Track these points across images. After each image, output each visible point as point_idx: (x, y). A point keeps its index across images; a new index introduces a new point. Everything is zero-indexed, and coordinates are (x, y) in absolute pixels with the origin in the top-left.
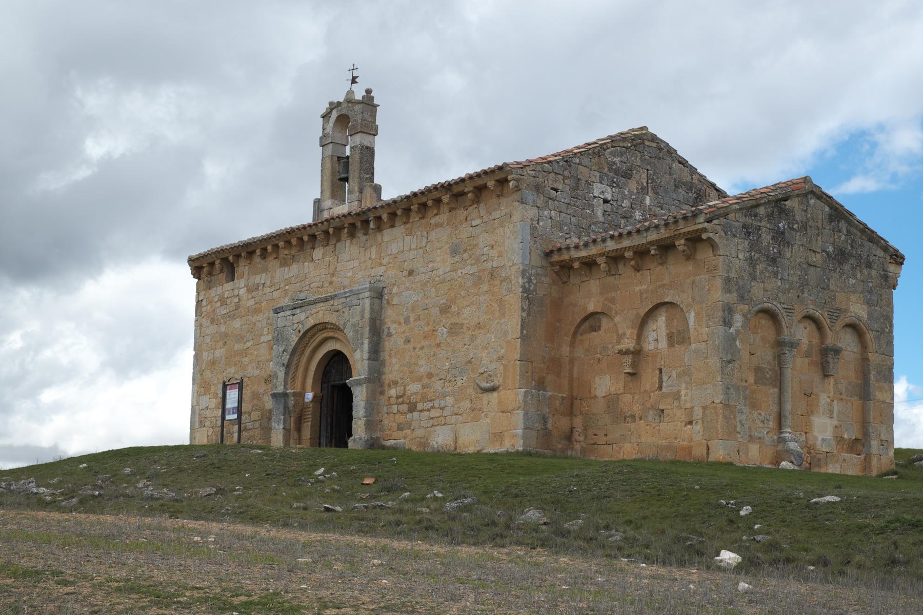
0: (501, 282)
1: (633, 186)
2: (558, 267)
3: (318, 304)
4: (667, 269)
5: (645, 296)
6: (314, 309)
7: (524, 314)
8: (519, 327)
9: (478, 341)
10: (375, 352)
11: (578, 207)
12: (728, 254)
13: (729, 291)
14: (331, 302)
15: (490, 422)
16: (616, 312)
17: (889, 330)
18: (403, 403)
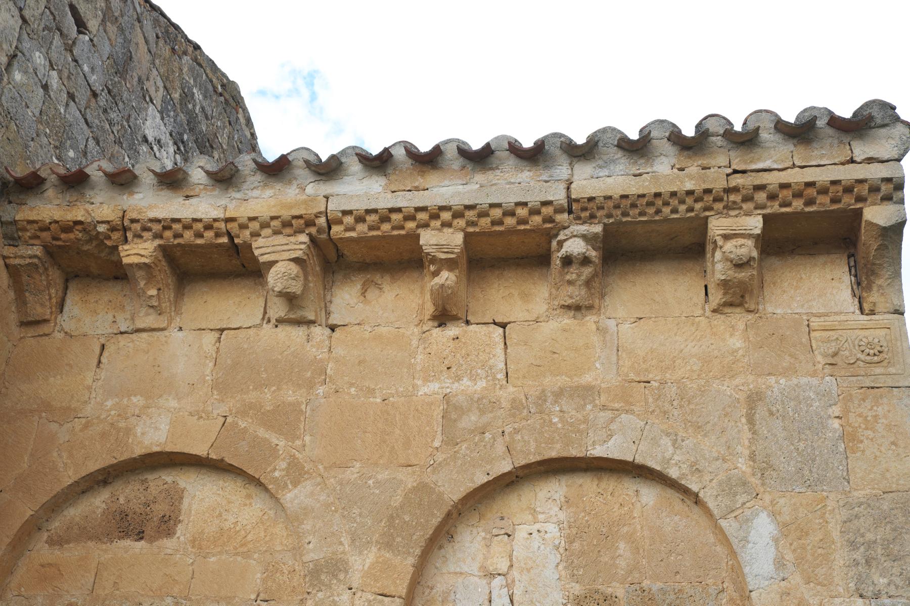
2: (37, 250)
4: (601, 330)
5: (472, 419)
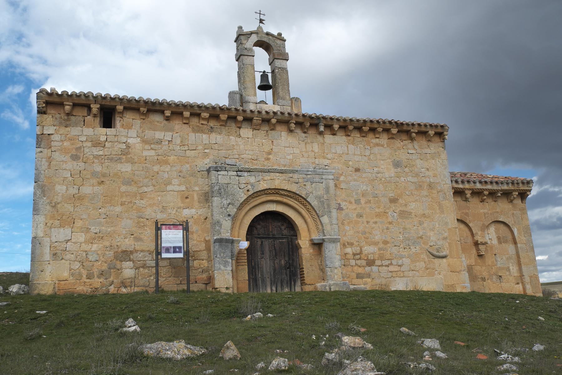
0: (438, 192)
3: (272, 173)
4: (498, 204)
6: (267, 177)
9: (425, 225)
14: (291, 175)
15: (443, 278)
16: (469, 221)
18: (360, 259)
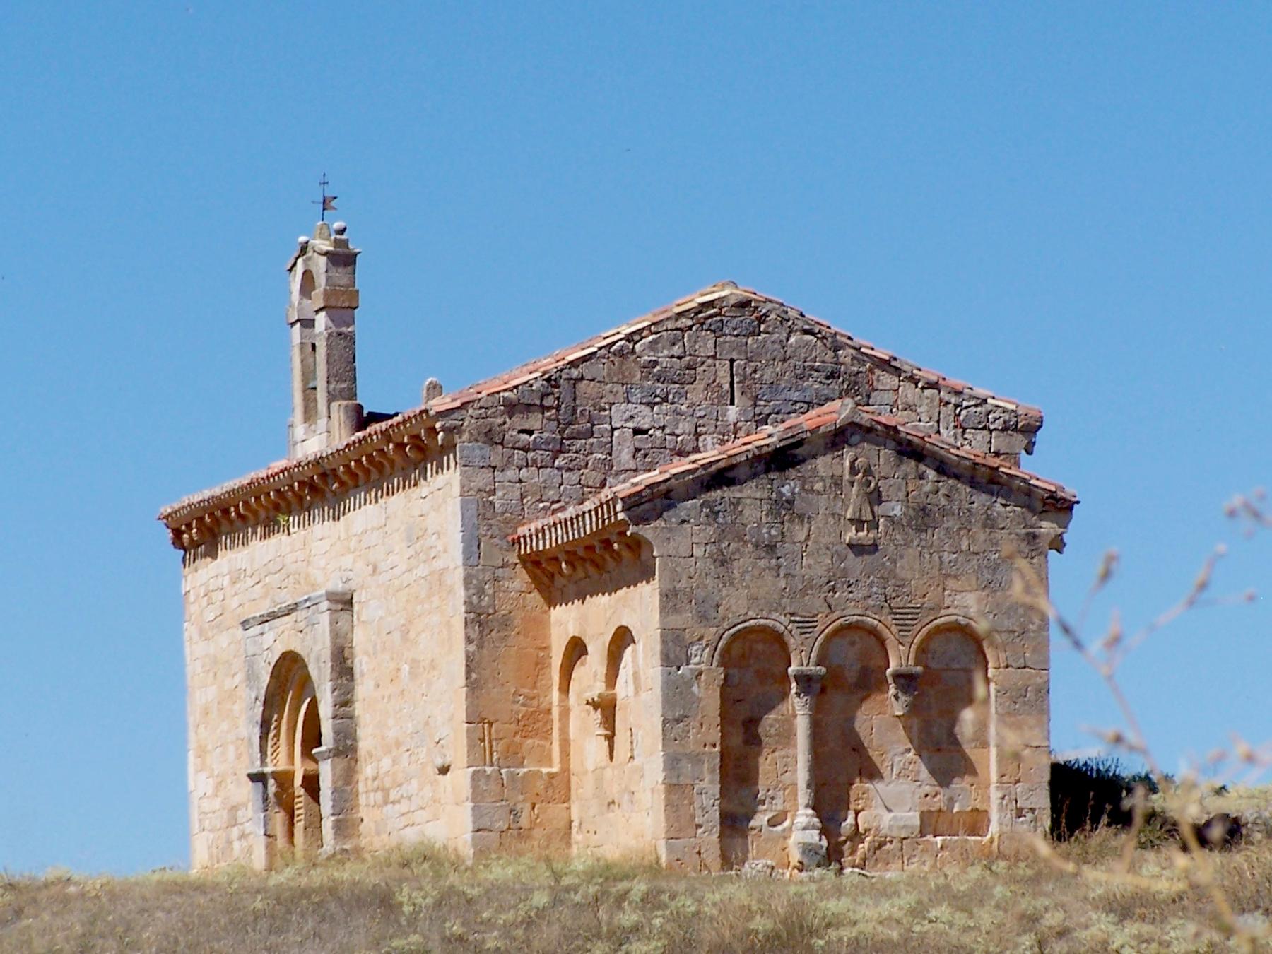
1: (696, 393)
7: (472, 648)
8: (463, 669)
10: (344, 702)
11: (577, 452)
12: (672, 552)
13: (675, 609)
17: (1039, 627)
